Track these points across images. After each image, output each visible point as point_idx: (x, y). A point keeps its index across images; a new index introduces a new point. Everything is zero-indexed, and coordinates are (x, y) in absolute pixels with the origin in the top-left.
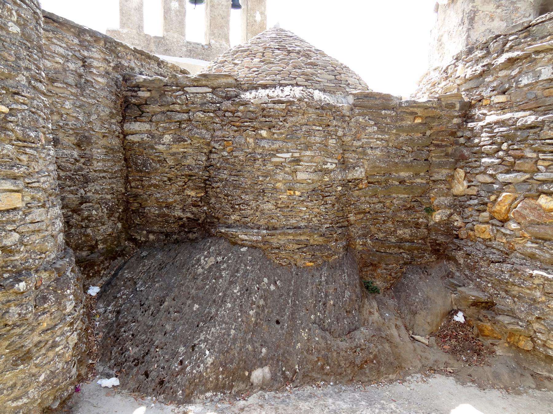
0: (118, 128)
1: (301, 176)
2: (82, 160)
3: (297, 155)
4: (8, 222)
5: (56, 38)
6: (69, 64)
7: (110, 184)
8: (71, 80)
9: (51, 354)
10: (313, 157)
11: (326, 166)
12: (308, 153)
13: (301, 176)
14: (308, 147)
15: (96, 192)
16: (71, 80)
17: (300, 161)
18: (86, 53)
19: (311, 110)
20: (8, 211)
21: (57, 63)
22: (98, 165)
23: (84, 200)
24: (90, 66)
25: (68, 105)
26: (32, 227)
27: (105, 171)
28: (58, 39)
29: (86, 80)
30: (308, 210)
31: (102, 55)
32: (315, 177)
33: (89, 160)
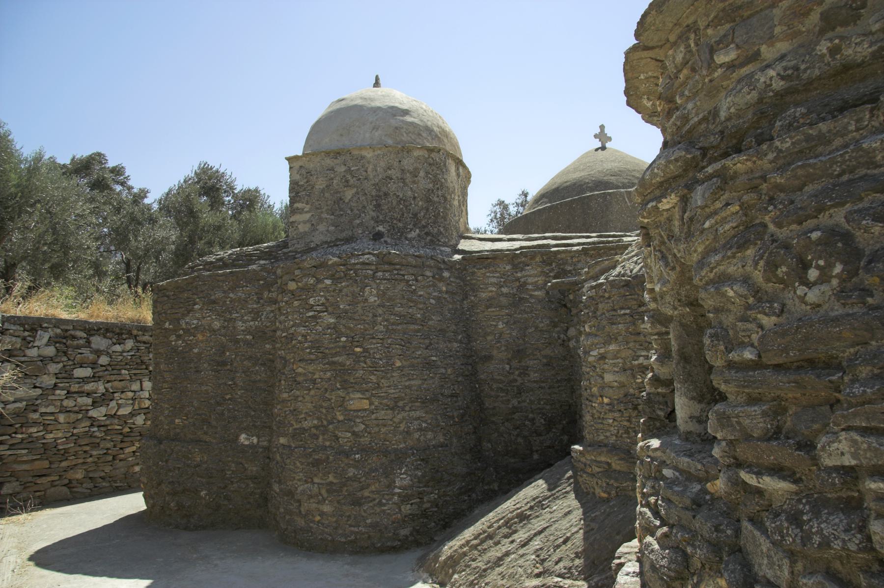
0: (562, 336)
1: (608, 378)
2: (517, 373)
3: (602, 351)
4: (357, 417)
5: (489, 272)
6: (503, 289)
7: (550, 394)
8: (504, 301)
9: (378, 510)
10: (619, 351)
11: (636, 362)
12: (612, 347)
13: (608, 378)
14: (611, 339)
15: (532, 402)
16: (504, 301)
17: (606, 358)
18: (519, 275)
19: (615, 291)
20: (360, 410)
21: (491, 291)
22: (534, 376)
23: (515, 410)
24: (525, 283)
25: (501, 325)
26: (374, 422)
27: (543, 382)
28: (493, 272)
29: (520, 298)
30: (616, 423)
31: (539, 269)
32: (622, 378)
33: (524, 372)
